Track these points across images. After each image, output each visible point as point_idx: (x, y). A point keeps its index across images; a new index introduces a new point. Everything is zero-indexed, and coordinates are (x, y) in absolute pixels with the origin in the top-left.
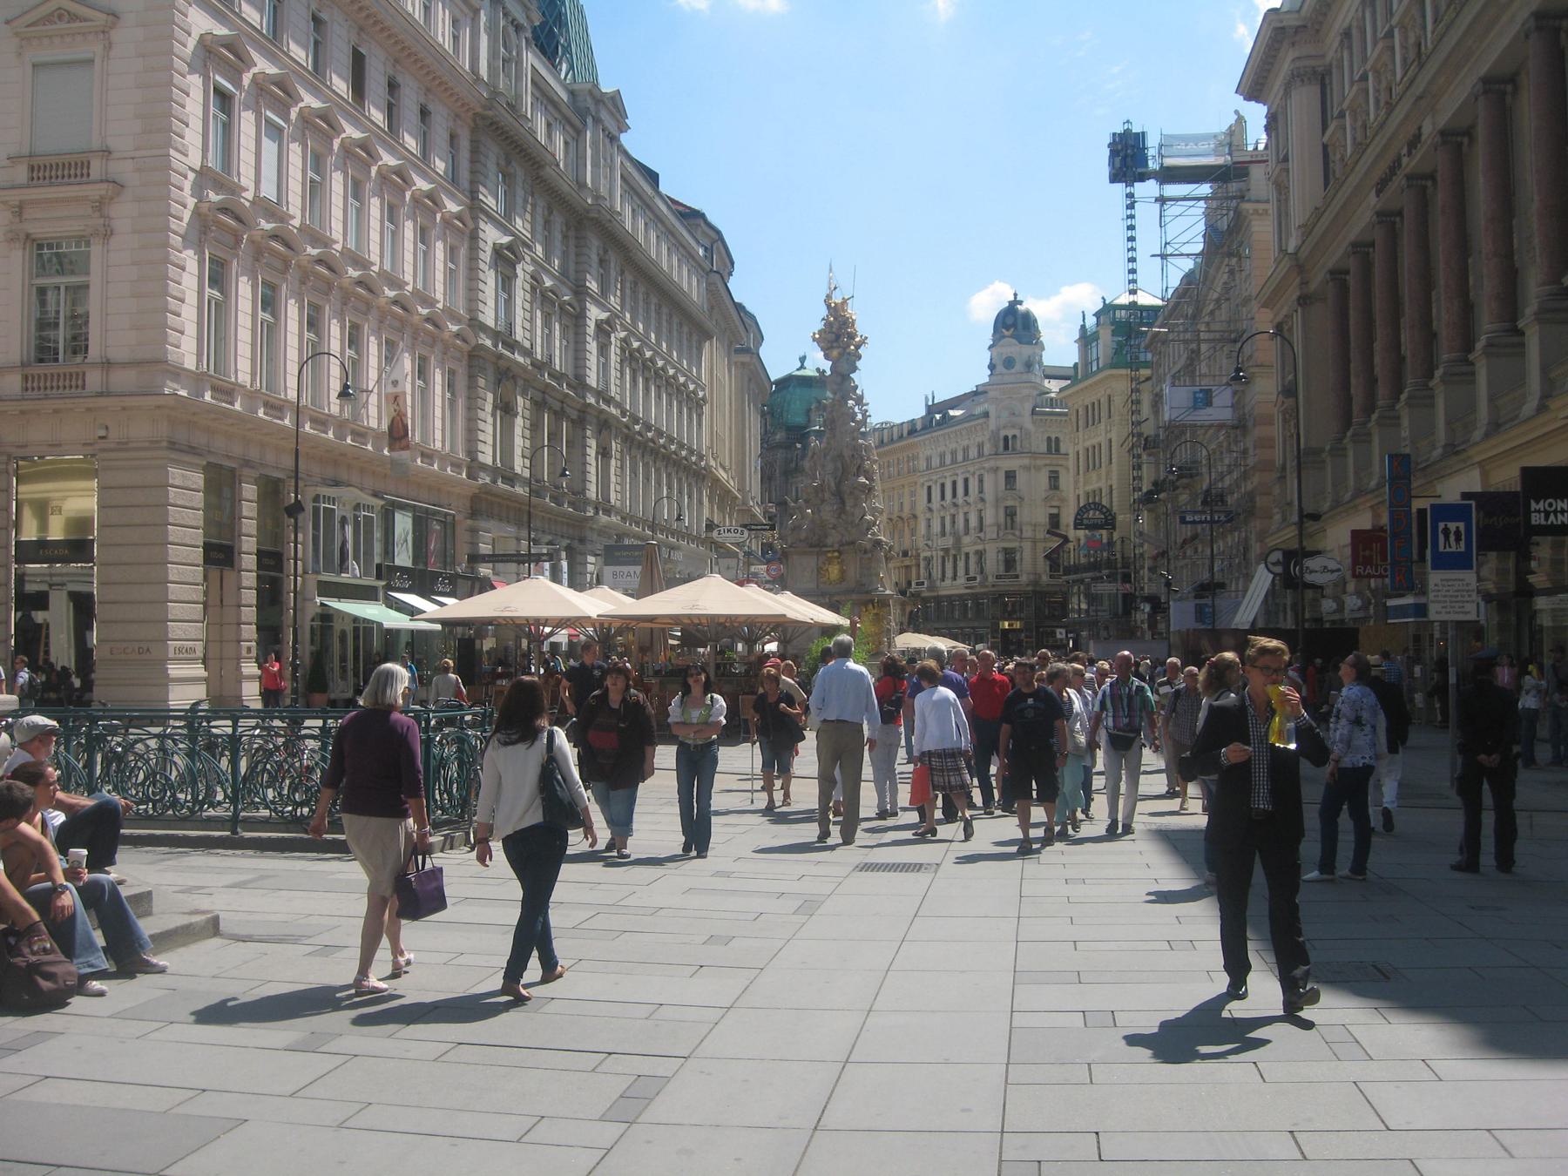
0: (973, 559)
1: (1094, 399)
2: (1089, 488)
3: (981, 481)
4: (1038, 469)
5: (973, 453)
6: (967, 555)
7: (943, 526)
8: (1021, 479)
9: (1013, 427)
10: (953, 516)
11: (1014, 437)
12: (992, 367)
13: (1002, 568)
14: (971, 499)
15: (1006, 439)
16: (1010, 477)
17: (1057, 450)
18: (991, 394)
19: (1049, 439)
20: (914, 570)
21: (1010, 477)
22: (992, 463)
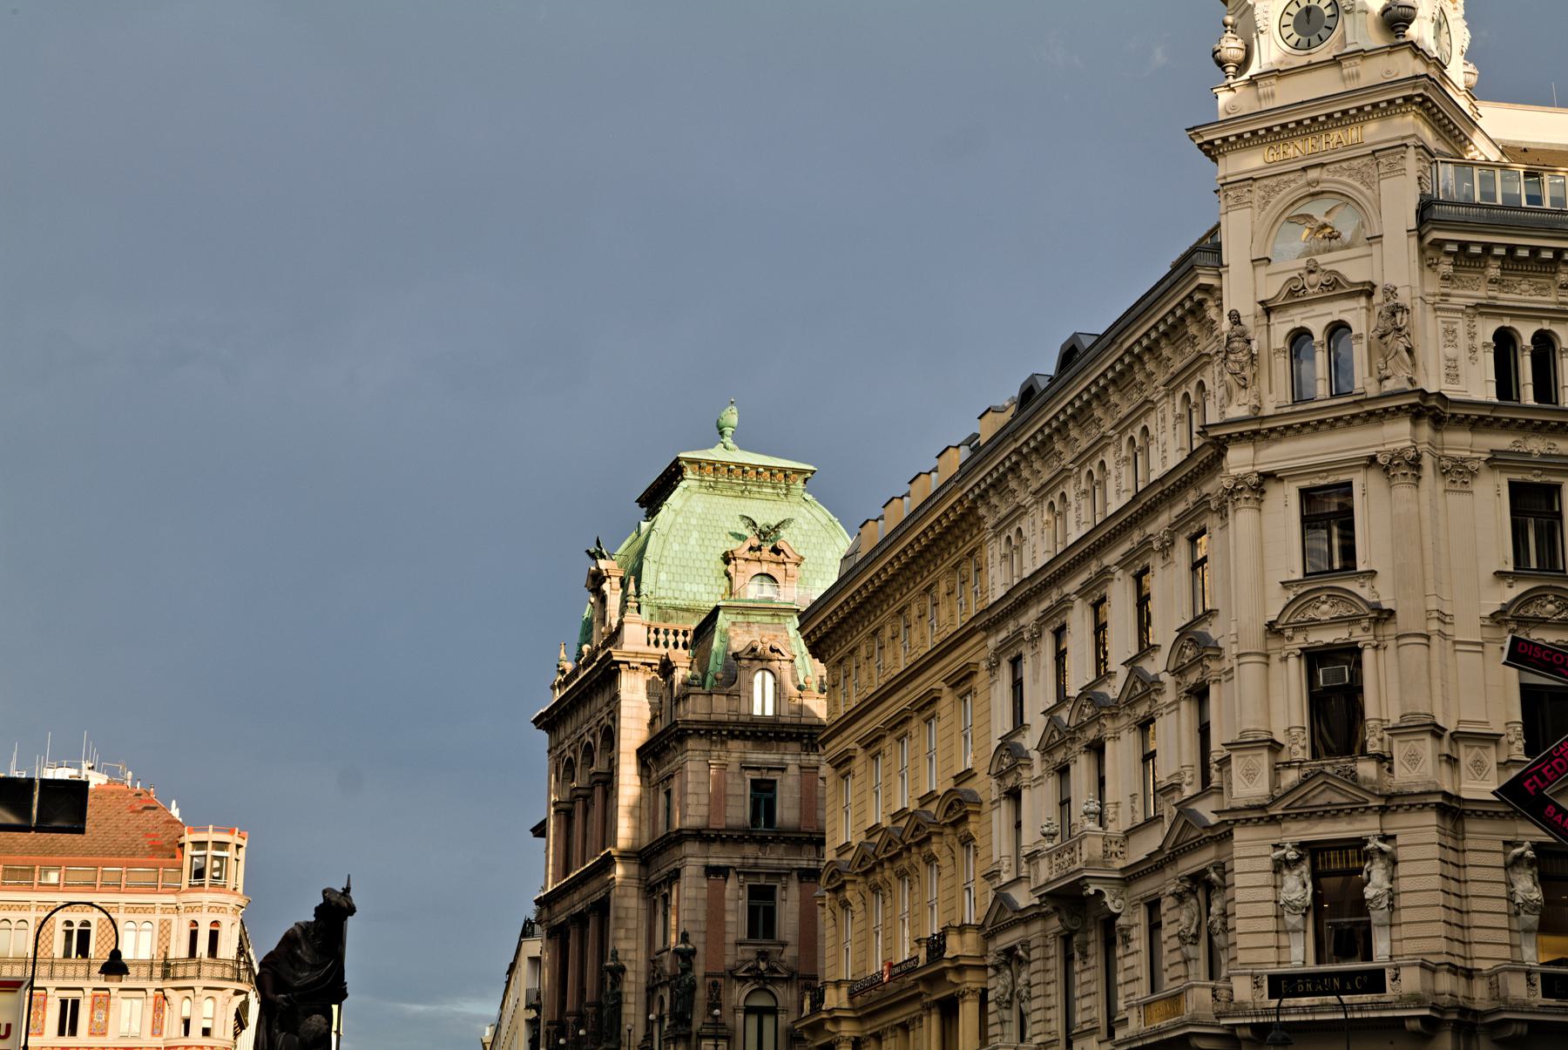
0: (1178, 919)
3: (1197, 565)
4: (1458, 472)
6: (1153, 905)
7: (1065, 803)
8: (1374, 508)
9: (1335, 288)
10: (1097, 749)
11: (1338, 329)
13: (1299, 955)
14: (1156, 666)
15: (1299, 336)
16: (1328, 511)
19: (1504, 342)
20: (968, 1012)
21: (1328, 511)
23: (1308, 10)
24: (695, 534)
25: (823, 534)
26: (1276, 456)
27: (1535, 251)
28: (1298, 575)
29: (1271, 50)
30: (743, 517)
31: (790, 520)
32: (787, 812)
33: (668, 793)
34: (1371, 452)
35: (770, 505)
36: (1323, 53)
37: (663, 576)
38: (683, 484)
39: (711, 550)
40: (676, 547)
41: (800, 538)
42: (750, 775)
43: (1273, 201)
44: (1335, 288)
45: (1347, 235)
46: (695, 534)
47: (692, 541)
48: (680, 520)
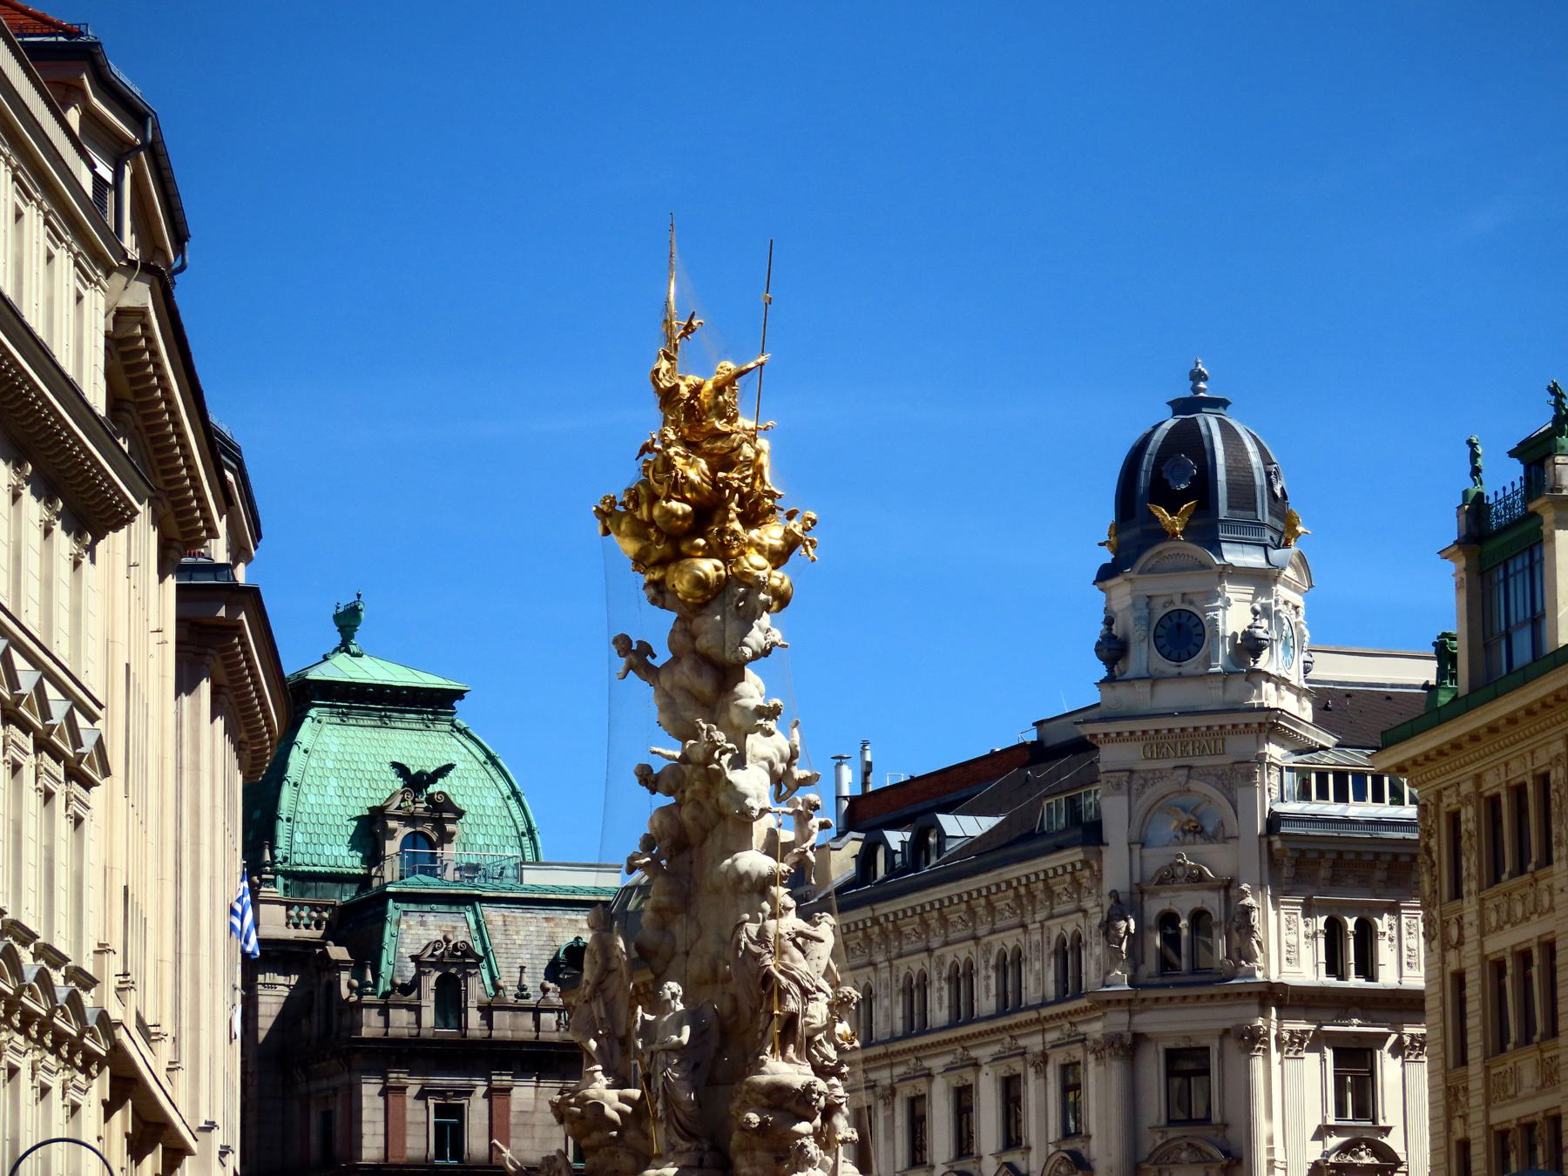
1: (1521, 771)
2: (1507, 1114)
3: (1071, 1086)
5: (1039, 979)
9: (1198, 879)
12: (1112, 649)
15: (1168, 920)
16: (1188, 1065)
17: (1367, 967)
18: (1110, 756)
22: (1118, 1021)
23: (1179, 626)
24: (333, 782)
25: (483, 774)
26: (1148, 1022)
27: (1359, 854)
28: (1163, 1121)
29: (1142, 656)
30: (395, 765)
31: (450, 767)
32: (476, 1142)
33: (327, 1117)
34: (1228, 1025)
35: (415, 736)
36: (1190, 666)
37: (298, 837)
38: (313, 712)
39: (353, 802)
40: (312, 799)
41: (456, 782)
42: (431, 1103)
43: (1149, 791)
44: (1198, 879)
45: (1209, 829)
46: (333, 782)
47: (331, 791)
48: (313, 763)
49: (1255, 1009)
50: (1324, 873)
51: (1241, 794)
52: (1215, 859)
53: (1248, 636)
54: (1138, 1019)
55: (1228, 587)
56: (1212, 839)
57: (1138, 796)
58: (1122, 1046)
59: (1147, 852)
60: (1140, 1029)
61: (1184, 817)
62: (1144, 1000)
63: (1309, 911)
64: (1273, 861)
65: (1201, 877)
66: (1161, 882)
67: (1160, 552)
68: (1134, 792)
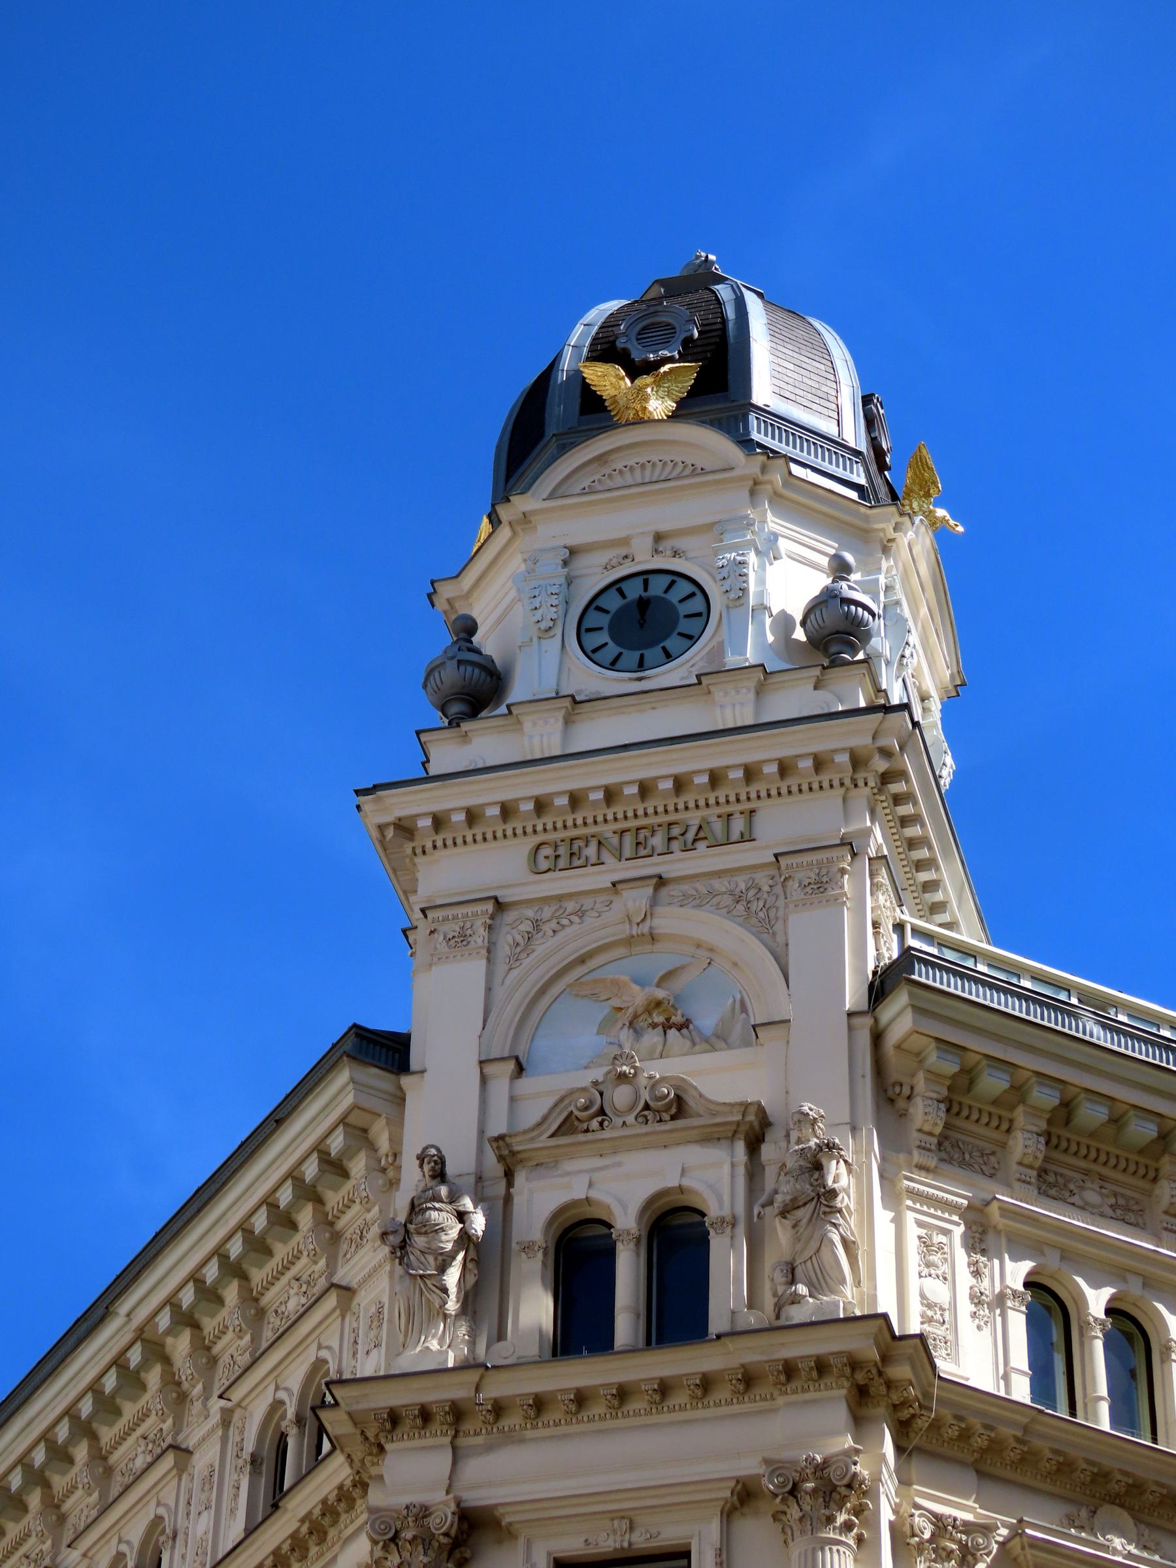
23: (643, 604)
34: (750, 1466)
43: (542, 946)
49: (839, 1413)
50: (1024, 1144)
51: (801, 926)
52: (724, 1079)
53: (828, 599)
54: (475, 1468)
55: (773, 523)
56: (718, 1040)
57: (515, 959)
58: (425, 1540)
59: (526, 1085)
60: (477, 1498)
61: (638, 997)
62: (498, 1409)
63: (982, 1237)
64: (889, 1097)
65: (679, 1107)
66: (568, 1126)
67: (602, 459)
68: (503, 950)
